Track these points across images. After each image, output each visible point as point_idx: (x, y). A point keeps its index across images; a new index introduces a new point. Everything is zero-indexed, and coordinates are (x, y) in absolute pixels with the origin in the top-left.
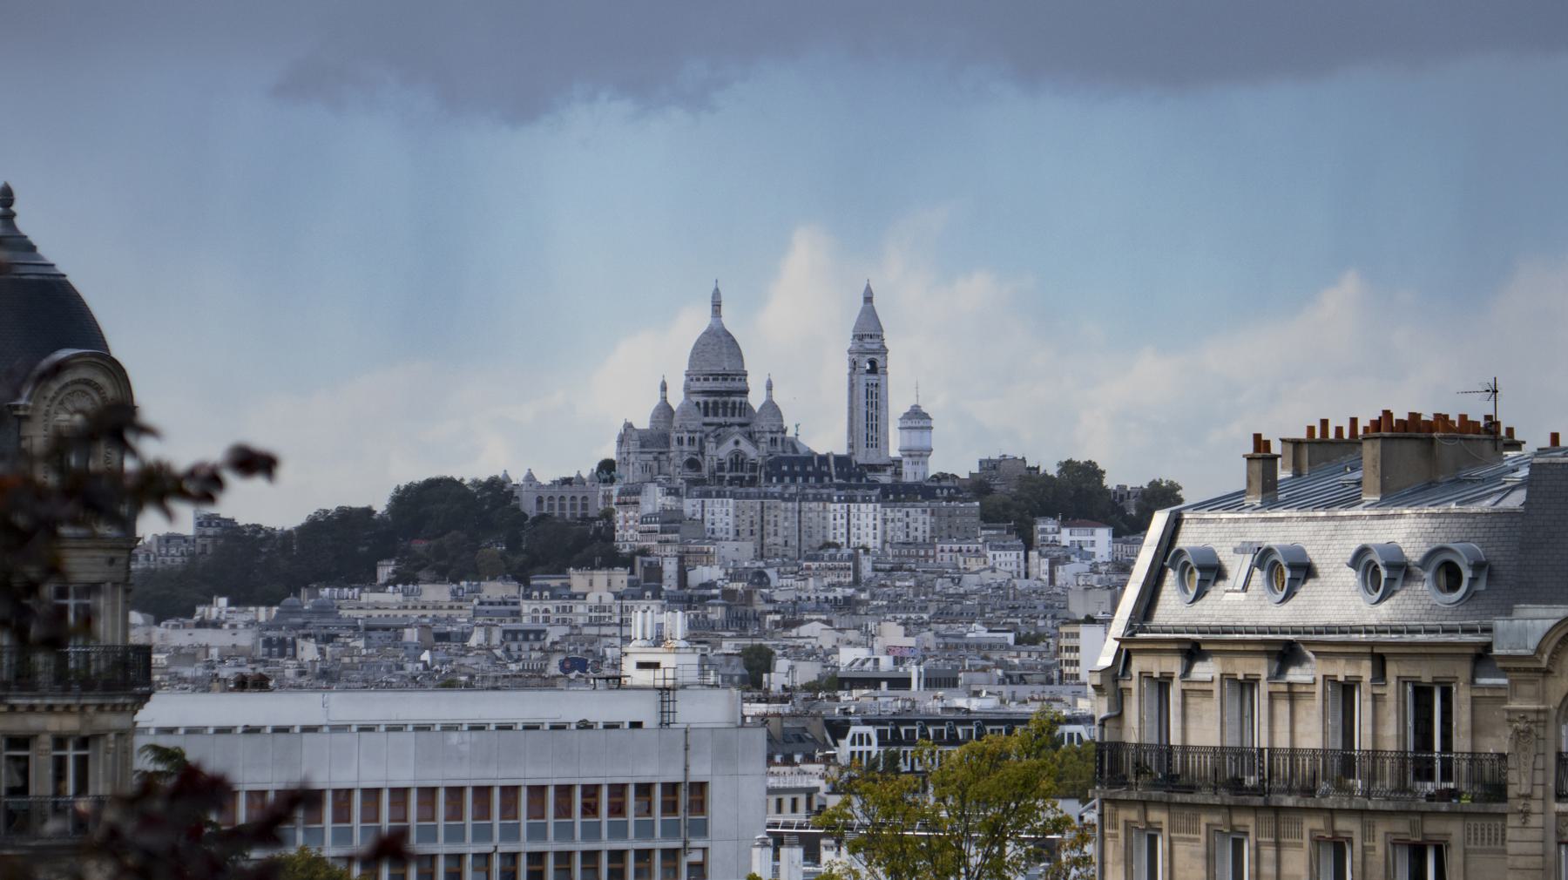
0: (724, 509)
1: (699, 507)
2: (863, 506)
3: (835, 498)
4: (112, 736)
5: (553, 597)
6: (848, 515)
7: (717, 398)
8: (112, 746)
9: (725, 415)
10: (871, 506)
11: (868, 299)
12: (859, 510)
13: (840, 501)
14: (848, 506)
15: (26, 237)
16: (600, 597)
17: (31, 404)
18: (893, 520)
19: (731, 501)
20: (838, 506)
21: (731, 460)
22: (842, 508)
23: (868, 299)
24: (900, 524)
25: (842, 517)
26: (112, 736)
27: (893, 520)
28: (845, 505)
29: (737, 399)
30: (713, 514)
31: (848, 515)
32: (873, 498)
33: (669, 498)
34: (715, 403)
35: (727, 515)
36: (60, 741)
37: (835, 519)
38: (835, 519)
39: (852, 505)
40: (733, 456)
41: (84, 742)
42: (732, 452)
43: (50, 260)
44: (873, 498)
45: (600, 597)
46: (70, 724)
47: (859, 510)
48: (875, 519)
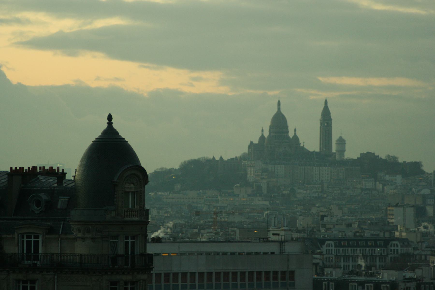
2: (324, 167)
3: (316, 165)
4: (142, 281)
8: (142, 284)
10: (327, 168)
11: (326, 102)
12: (323, 169)
14: (320, 168)
15: (124, 139)
17: (118, 181)
19: (283, 166)
23: (326, 102)
26: (142, 281)
27: (334, 172)
32: (328, 165)
36: (126, 283)
37: (316, 171)
38: (316, 171)
39: (321, 167)
41: (133, 283)
43: (123, 137)
44: (328, 165)
46: (129, 278)
47: (323, 169)
48: (328, 172)
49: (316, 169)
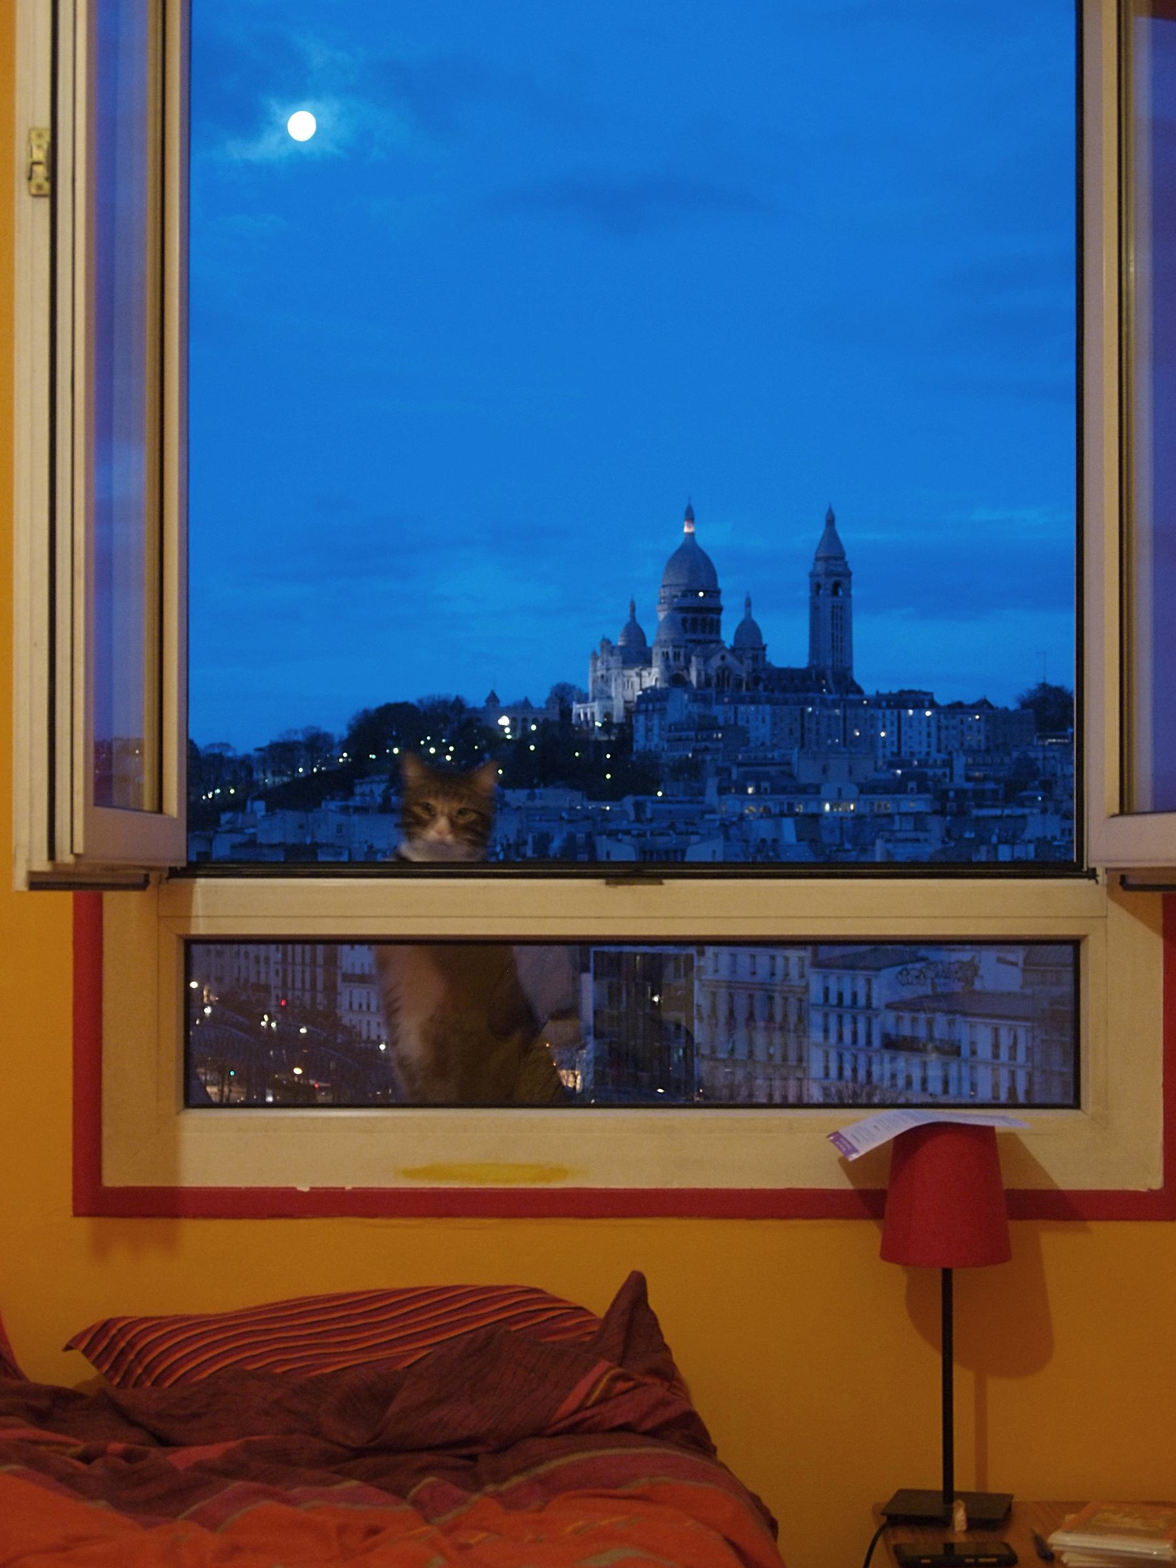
0: (760, 717)
1: (731, 714)
5: (774, 791)
6: (899, 722)
7: (696, 615)
9: (703, 632)
13: (888, 707)
16: (840, 790)
18: (947, 728)
20: (888, 712)
21: (718, 676)
22: (892, 713)
24: (954, 732)
25: (892, 724)
27: (947, 728)
28: (896, 712)
29: (714, 616)
30: (747, 722)
31: (899, 722)
33: (696, 705)
34: (694, 621)
35: (764, 721)
40: (720, 672)
42: (719, 668)
45: (840, 790)
49: (884, 716)
